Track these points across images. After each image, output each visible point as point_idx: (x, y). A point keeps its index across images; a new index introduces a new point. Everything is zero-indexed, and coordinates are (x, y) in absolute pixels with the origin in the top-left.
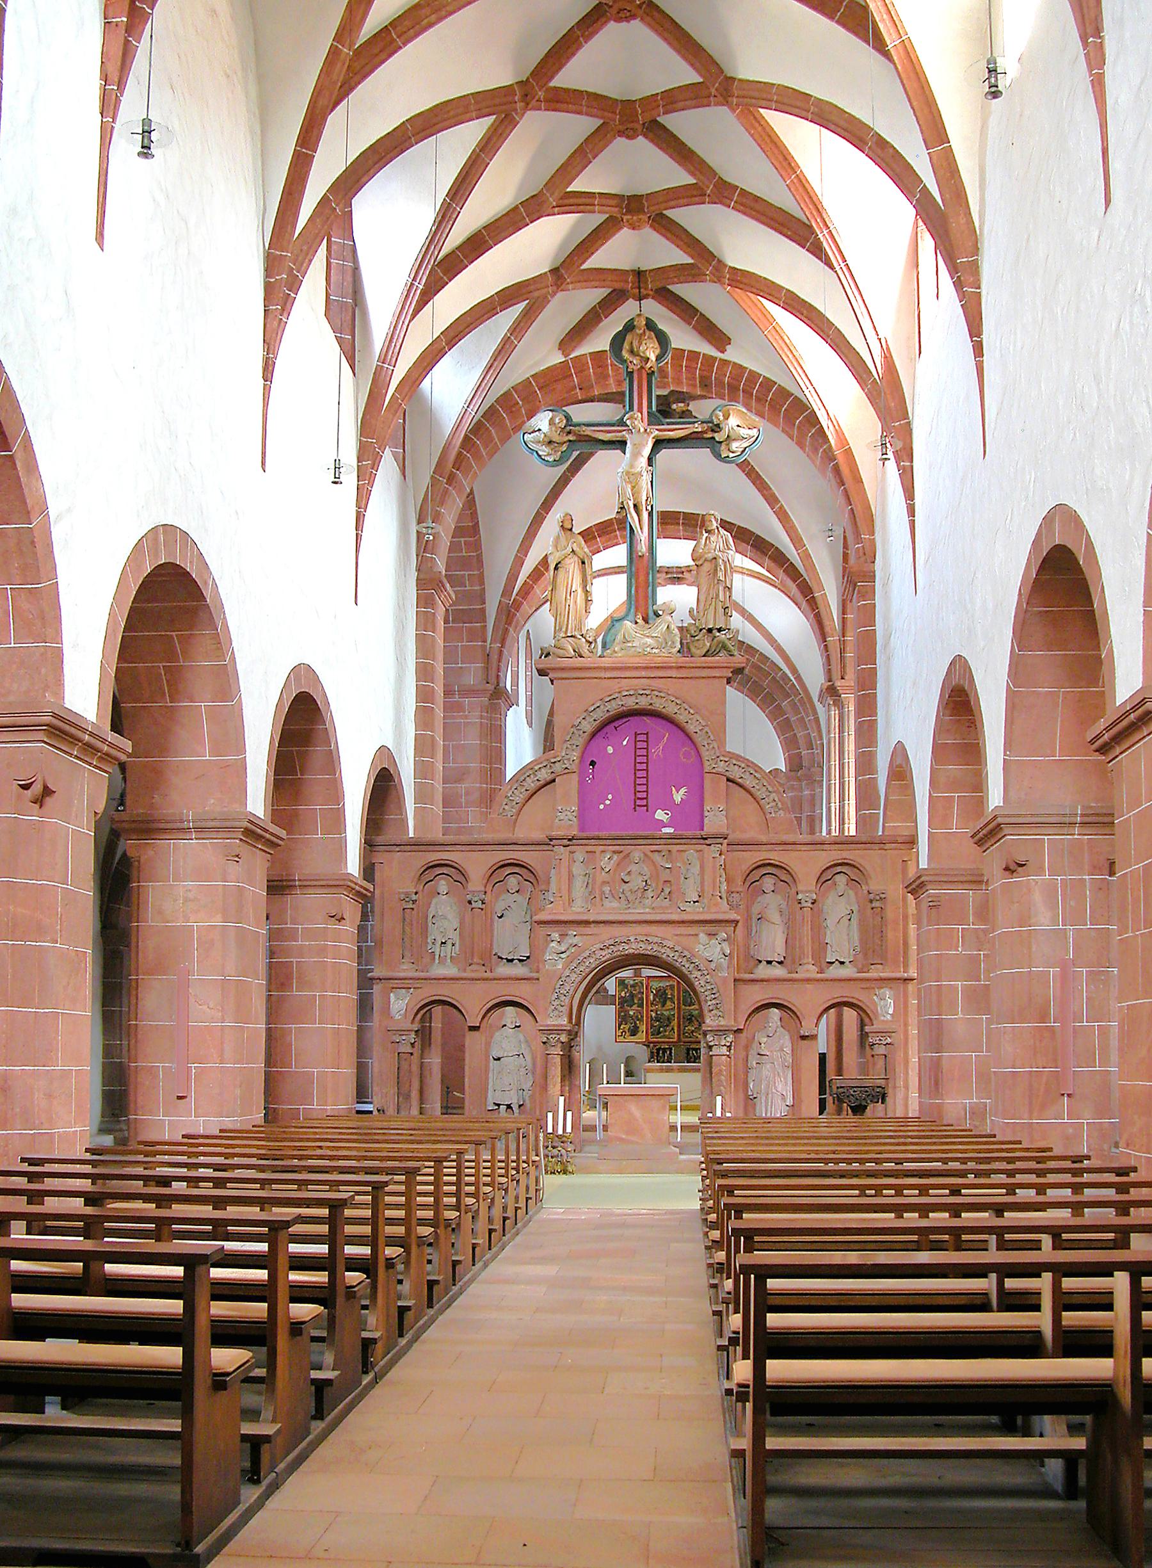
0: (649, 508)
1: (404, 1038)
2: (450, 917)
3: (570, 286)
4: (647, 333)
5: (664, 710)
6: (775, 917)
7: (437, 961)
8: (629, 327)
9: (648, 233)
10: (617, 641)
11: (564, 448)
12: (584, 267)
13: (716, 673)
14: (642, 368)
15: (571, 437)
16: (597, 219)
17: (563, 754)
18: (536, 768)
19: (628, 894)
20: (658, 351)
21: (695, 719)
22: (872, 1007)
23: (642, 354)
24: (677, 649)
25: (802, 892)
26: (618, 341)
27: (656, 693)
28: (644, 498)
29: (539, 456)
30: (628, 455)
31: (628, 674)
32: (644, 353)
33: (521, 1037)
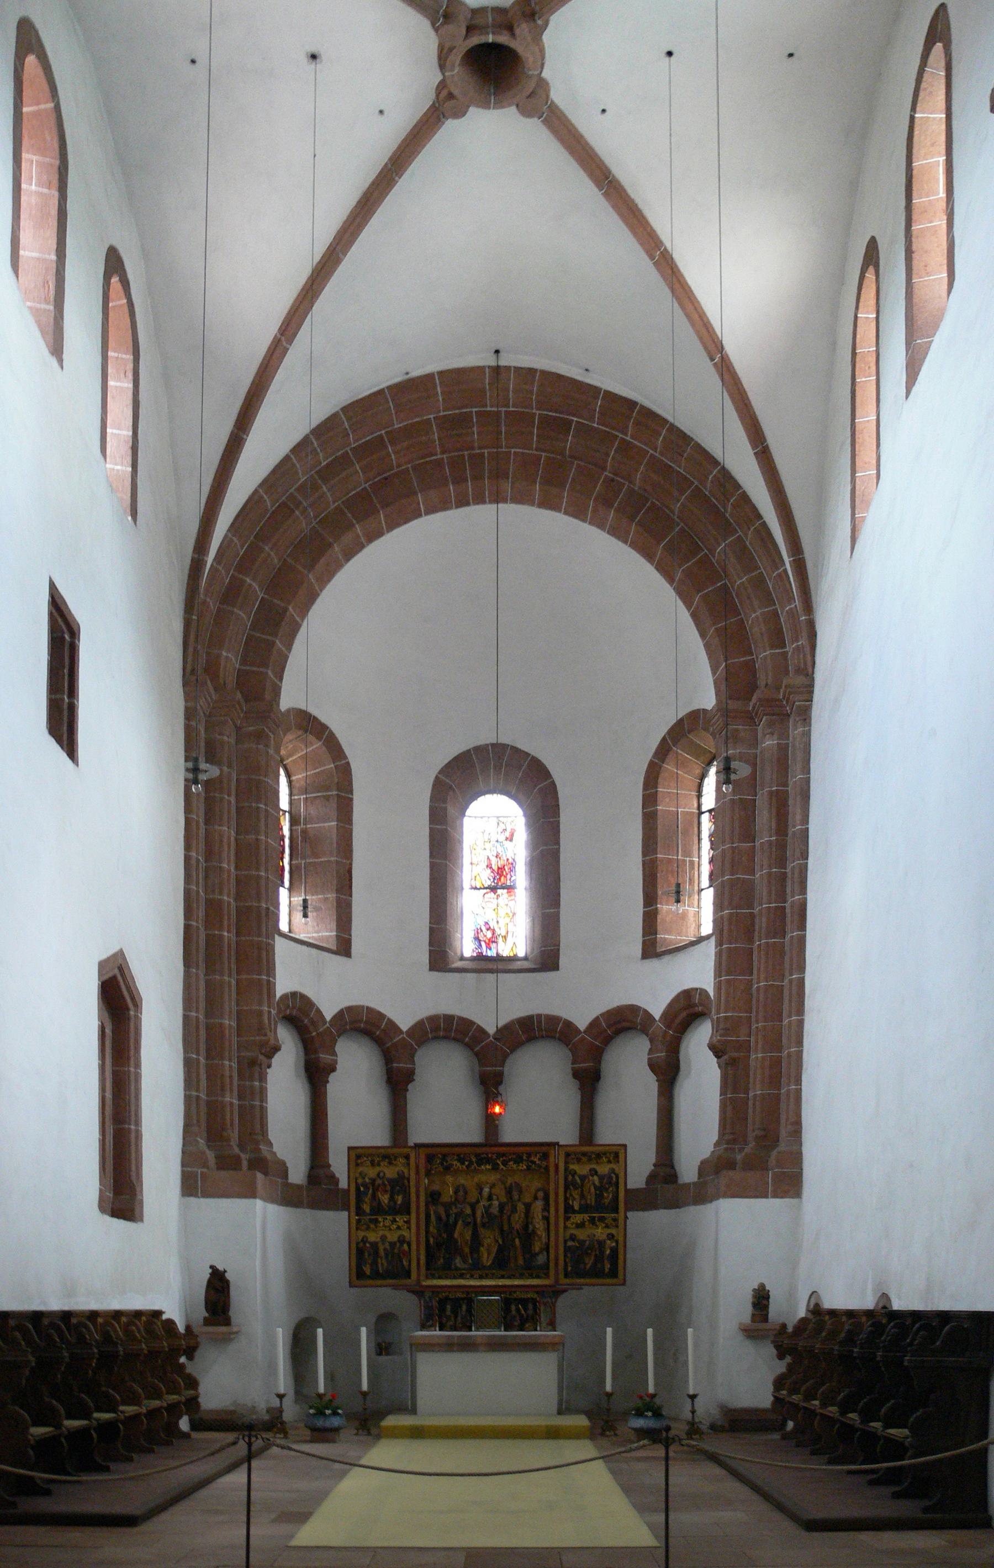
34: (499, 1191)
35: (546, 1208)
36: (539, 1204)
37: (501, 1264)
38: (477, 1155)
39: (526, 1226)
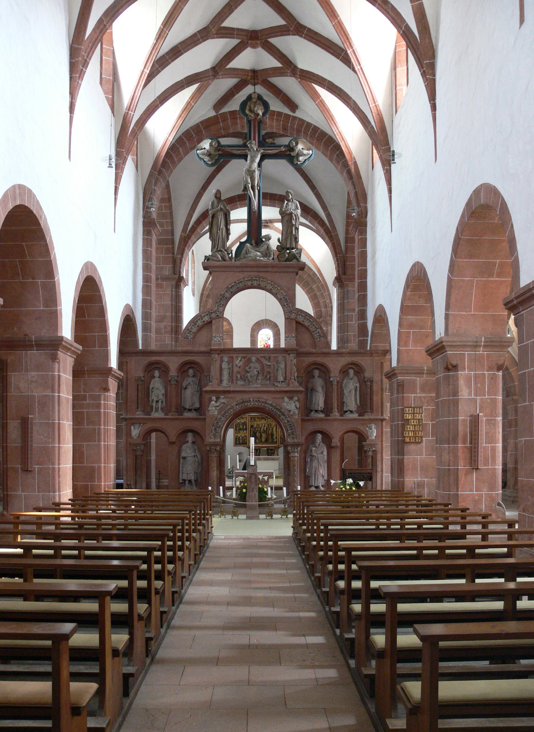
0: (258, 188)
1: (138, 448)
2: (160, 388)
3: (221, 77)
4: (258, 101)
6: (320, 389)
7: (154, 410)
8: (249, 98)
9: (260, 50)
10: (242, 253)
11: (217, 158)
12: (228, 67)
13: (291, 270)
14: (255, 119)
15: (220, 152)
16: (235, 42)
17: (216, 309)
18: (203, 315)
19: (249, 378)
20: (263, 111)
21: (280, 293)
22: (365, 433)
23: (255, 112)
24: (272, 258)
25: (332, 377)
26: (244, 105)
28: (256, 183)
29: (205, 161)
30: (248, 162)
32: (256, 111)
33: (196, 447)
34: (266, 425)
35: (276, 429)
36: (275, 428)
37: (266, 441)
38: (262, 417)
39: (272, 433)
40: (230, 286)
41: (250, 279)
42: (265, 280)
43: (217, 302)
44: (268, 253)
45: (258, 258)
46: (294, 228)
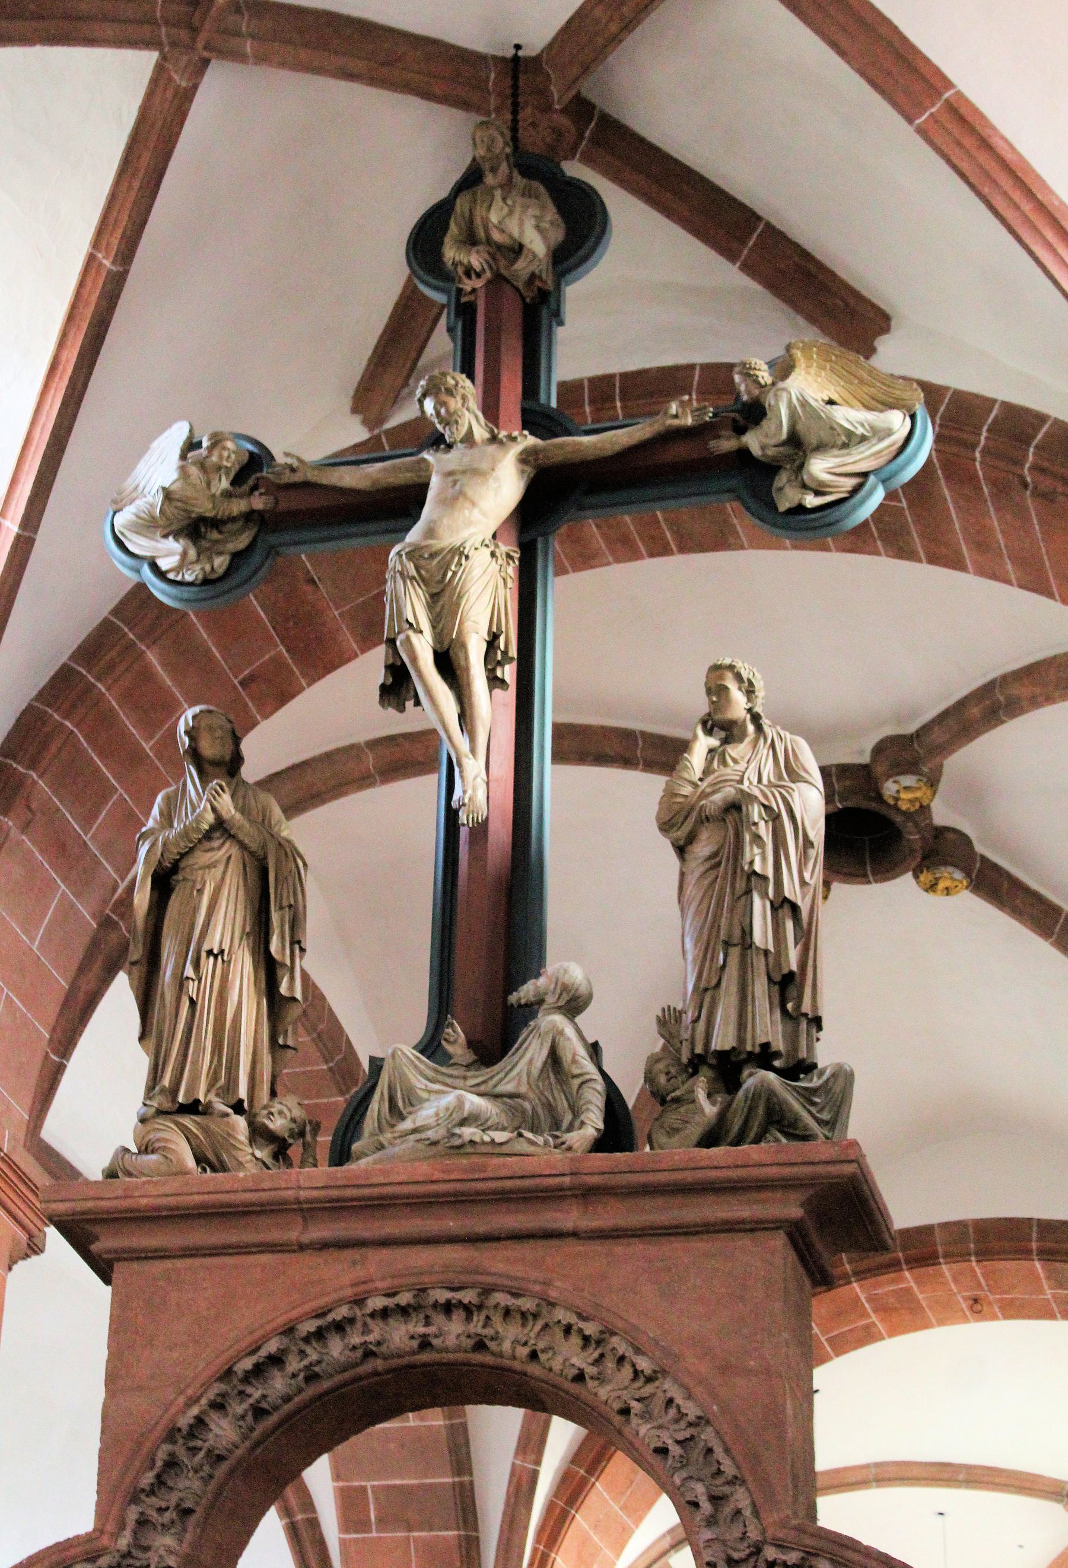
5: (533, 1369)
21: (659, 1402)
27: (501, 1298)
31: (392, 1227)
40: (247, 1364)
41: (405, 1298)
42: (527, 1304)
43: (135, 1496)
44: (562, 1104)
45: (469, 1132)
46: (760, 907)
